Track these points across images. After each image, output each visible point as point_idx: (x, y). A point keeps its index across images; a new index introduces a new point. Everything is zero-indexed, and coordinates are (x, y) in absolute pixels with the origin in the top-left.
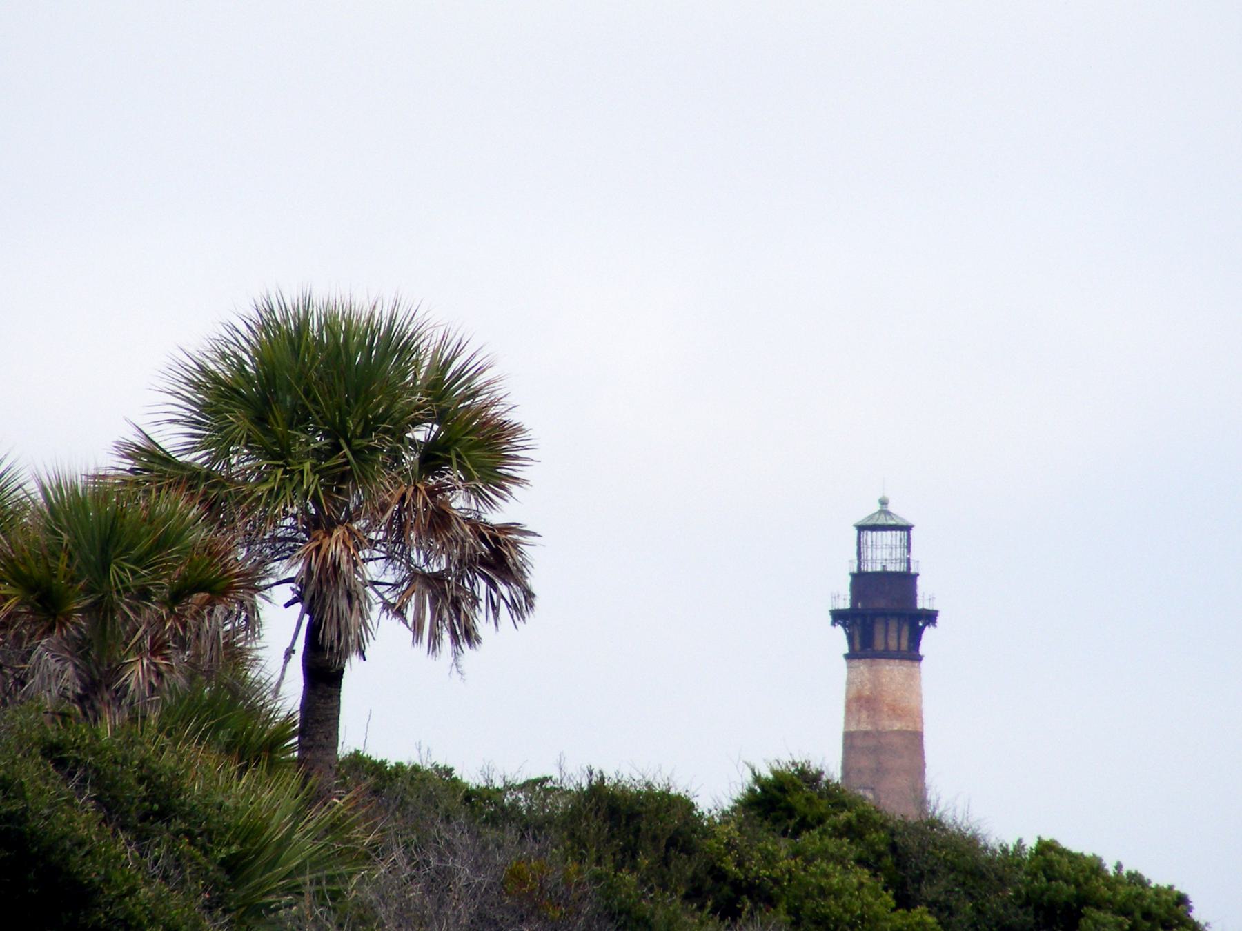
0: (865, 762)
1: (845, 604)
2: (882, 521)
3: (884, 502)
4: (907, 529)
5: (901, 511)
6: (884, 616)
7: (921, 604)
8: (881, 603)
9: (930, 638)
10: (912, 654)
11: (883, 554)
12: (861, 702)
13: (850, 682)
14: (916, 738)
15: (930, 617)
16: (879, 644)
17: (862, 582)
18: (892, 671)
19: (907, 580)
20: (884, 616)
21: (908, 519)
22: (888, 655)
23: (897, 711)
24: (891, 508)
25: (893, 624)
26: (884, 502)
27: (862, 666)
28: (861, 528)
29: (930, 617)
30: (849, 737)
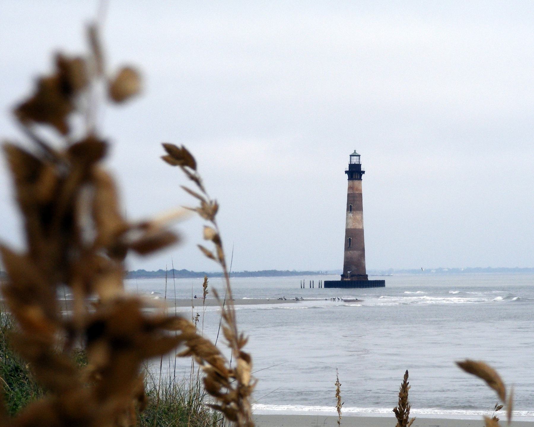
3: (355, 151)
4: (359, 156)
5: (358, 152)
6: (355, 172)
8: (354, 170)
9: (363, 176)
10: (360, 179)
11: (355, 160)
12: (350, 188)
14: (361, 195)
15: (364, 172)
16: (354, 177)
17: (351, 166)
18: (356, 182)
19: (359, 166)
20: (355, 172)
21: (359, 154)
22: (356, 179)
26: (355, 151)
27: (351, 181)
28: (351, 156)
29: (364, 172)
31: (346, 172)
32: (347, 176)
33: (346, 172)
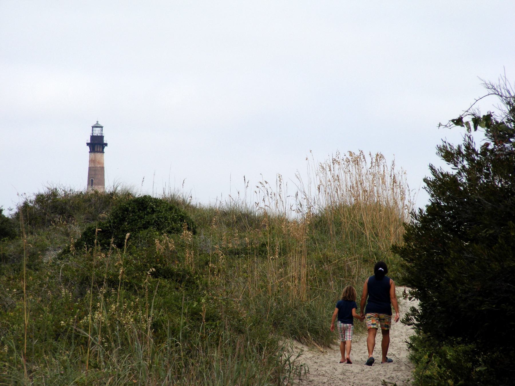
0: (93, 173)
1: (89, 142)
2: (97, 125)
3: (97, 122)
4: (102, 127)
5: (101, 124)
6: (97, 144)
7: (105, 142)
8: (96, 142)
9: (106, 149)
10: (103, 152)
11: (97, 132)
12: (92, 161)
13: (90, 157)
14: (103, 168)
15: (106, 145)
16: (96, 150)
17: (93, 137)
18: (98, 155)
19: (101, 137)
20: (97, 144)
21: (102, 125)
22: (97, 152)
23: (99, 163)
24: (99, 123)
25: (99, 146)
26: (97, 122)
27: (92, 154)
28: (93, 127)
29: (106, 145)
30: (90, 169)
31: (88, 144)
32: (88, 149)
33: (88, 144)
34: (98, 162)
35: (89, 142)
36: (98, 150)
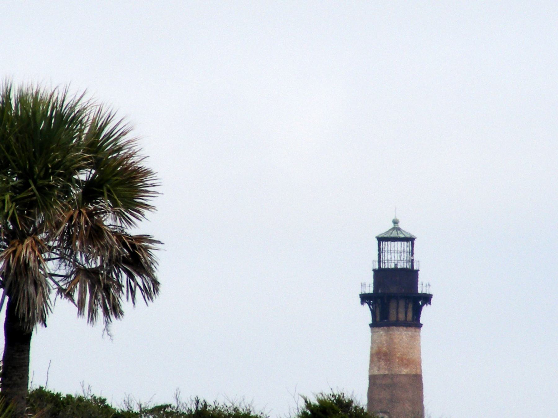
1: (370, 290)
2: (394, 234)
3: (395, 222)
4: (411, 240)
5: (407, 228)
6: (396, 298)
7: (421, 289)
8: (393, 290)
10: (416, 324)
11: (396, 255)
12: (379, 355)
13: (373, 342)
14: (417, 380)
15: (427, 299)
16: (393, 318)
17: (382, 275)
18: (401, 335)
19: (409, 275)
20: (396, 298)
22: (398, 324)
24: (400, 225)
25: (402, 303)
26: (395, 222)
27: (381, 332)
28: (381, 239)
29: (427, 299)
30: (373, 379)
31: (365, 298)
32: (365, 313)
33: (365, 298)
34: (402, 359)
35: (370, 290)
36: (402, 317)
